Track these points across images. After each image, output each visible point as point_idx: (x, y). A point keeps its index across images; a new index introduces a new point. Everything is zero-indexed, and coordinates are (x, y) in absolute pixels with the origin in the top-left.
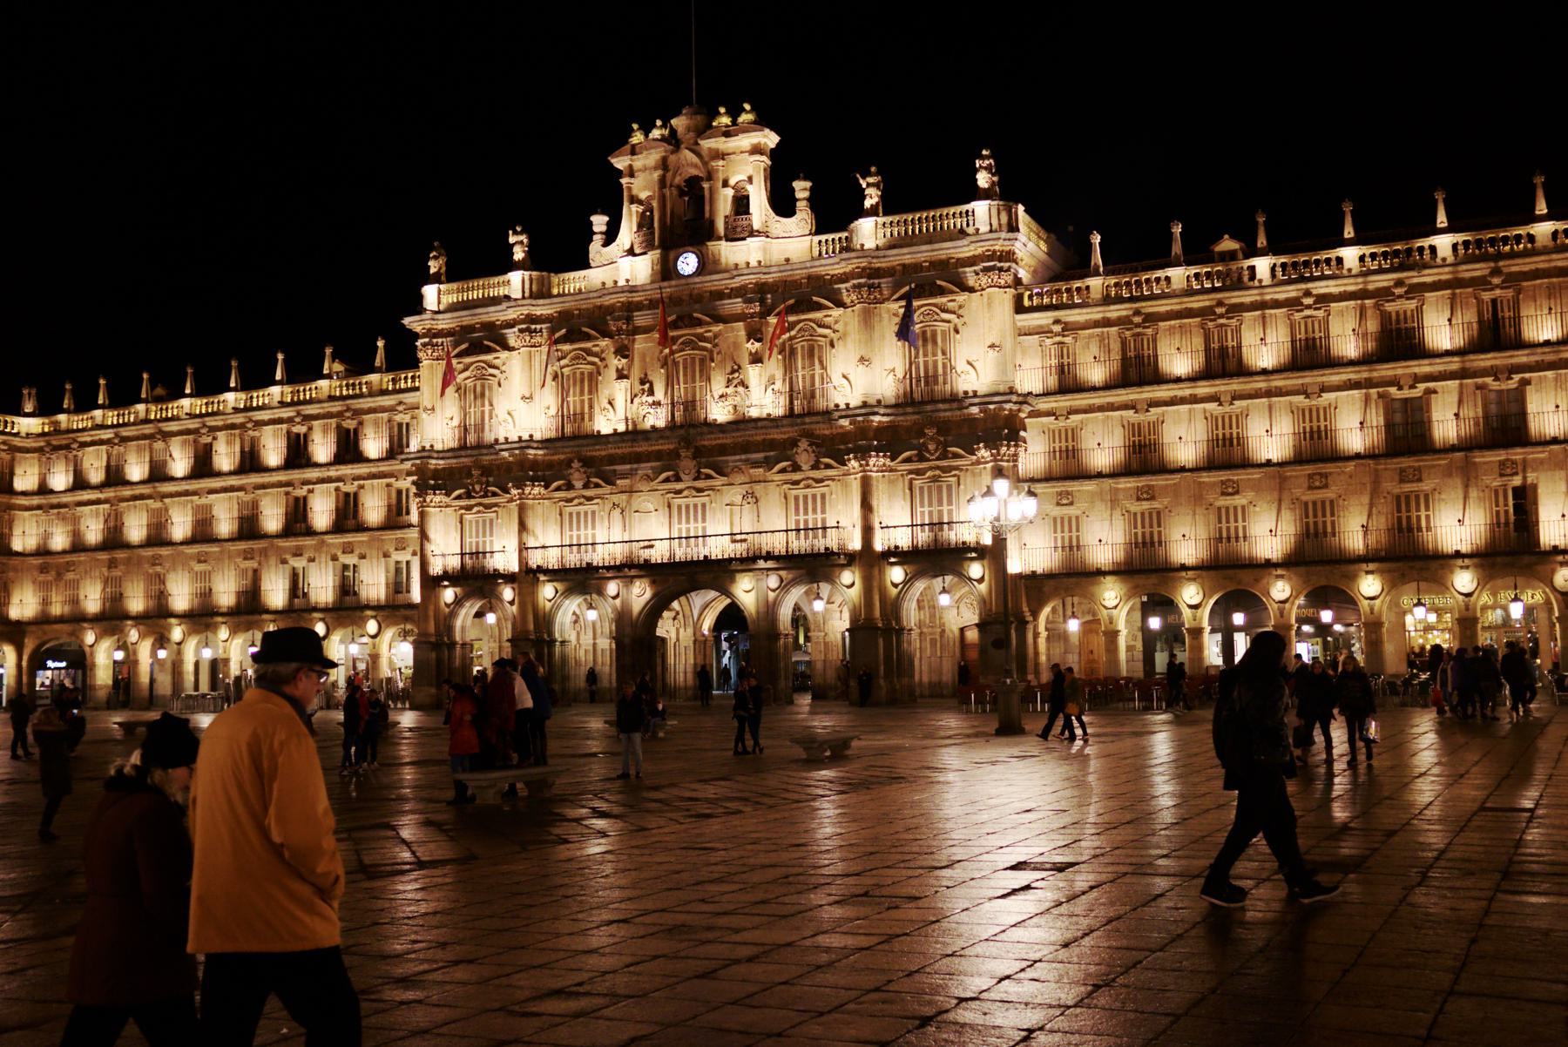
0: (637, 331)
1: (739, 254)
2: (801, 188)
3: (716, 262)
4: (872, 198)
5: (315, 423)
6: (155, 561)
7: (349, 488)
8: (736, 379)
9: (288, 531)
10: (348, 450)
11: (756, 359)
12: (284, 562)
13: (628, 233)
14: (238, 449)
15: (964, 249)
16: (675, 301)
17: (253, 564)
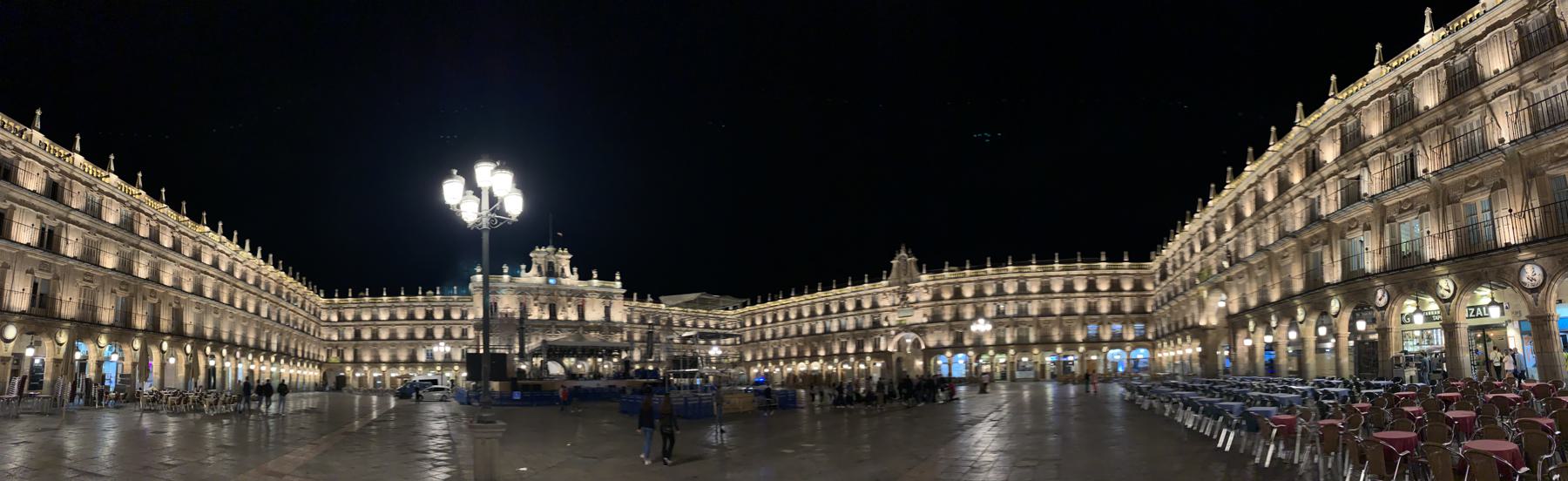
0: (539, 295)
1: (563, 281)
2: (575, 269)
3: (560, 281)
4: (595, 276)
5: (435, 308)
6: (374, 345)
7: (446, 327)
8: (564, 310)
9: (425, 339)
10: (447, 316)
11: (570, 306)
12: (424, 347)
13: (534, 270)
14: (406, 313)
15: (615, 291)
16: (549, 289)
17: (412, 348)
